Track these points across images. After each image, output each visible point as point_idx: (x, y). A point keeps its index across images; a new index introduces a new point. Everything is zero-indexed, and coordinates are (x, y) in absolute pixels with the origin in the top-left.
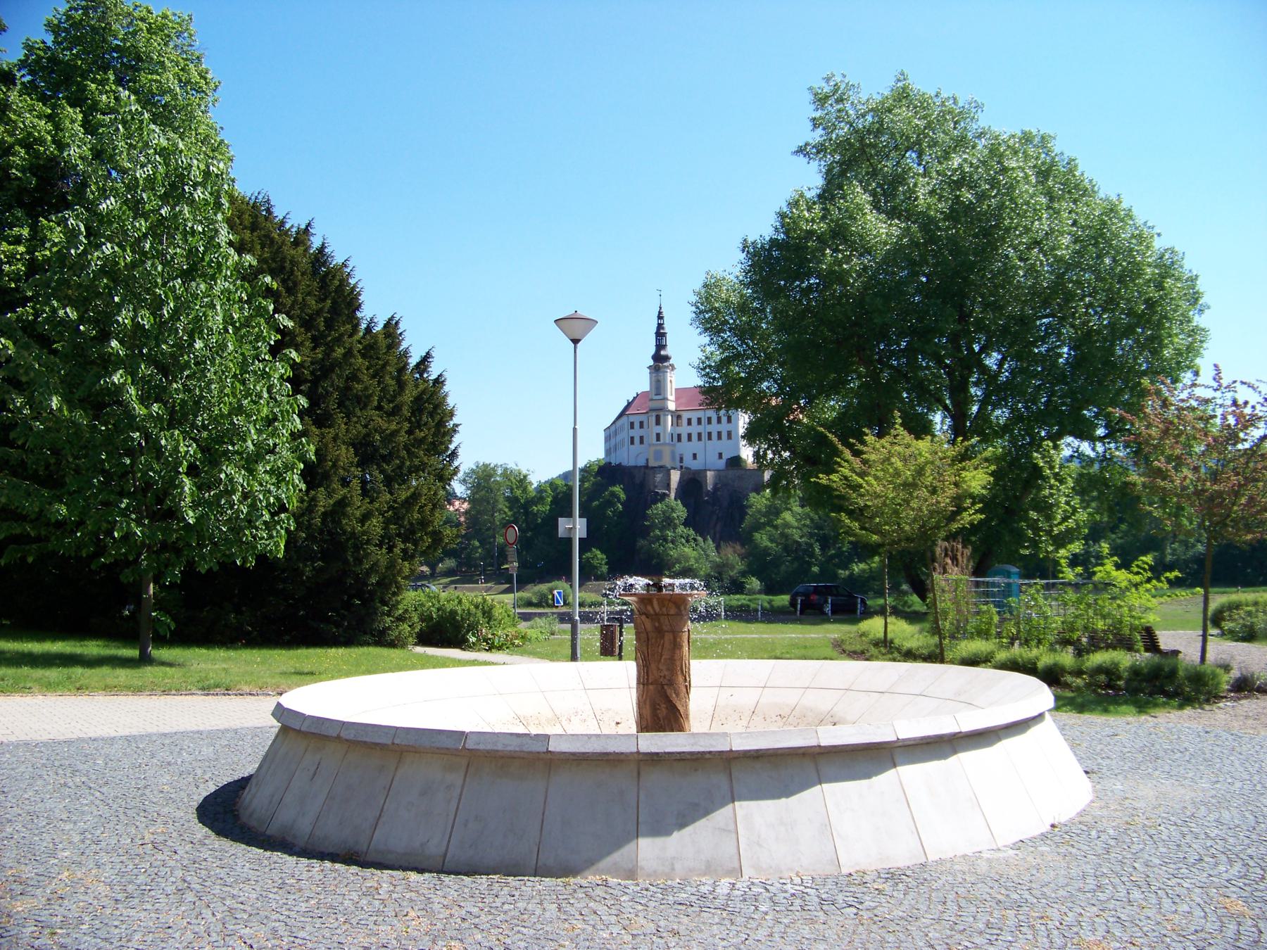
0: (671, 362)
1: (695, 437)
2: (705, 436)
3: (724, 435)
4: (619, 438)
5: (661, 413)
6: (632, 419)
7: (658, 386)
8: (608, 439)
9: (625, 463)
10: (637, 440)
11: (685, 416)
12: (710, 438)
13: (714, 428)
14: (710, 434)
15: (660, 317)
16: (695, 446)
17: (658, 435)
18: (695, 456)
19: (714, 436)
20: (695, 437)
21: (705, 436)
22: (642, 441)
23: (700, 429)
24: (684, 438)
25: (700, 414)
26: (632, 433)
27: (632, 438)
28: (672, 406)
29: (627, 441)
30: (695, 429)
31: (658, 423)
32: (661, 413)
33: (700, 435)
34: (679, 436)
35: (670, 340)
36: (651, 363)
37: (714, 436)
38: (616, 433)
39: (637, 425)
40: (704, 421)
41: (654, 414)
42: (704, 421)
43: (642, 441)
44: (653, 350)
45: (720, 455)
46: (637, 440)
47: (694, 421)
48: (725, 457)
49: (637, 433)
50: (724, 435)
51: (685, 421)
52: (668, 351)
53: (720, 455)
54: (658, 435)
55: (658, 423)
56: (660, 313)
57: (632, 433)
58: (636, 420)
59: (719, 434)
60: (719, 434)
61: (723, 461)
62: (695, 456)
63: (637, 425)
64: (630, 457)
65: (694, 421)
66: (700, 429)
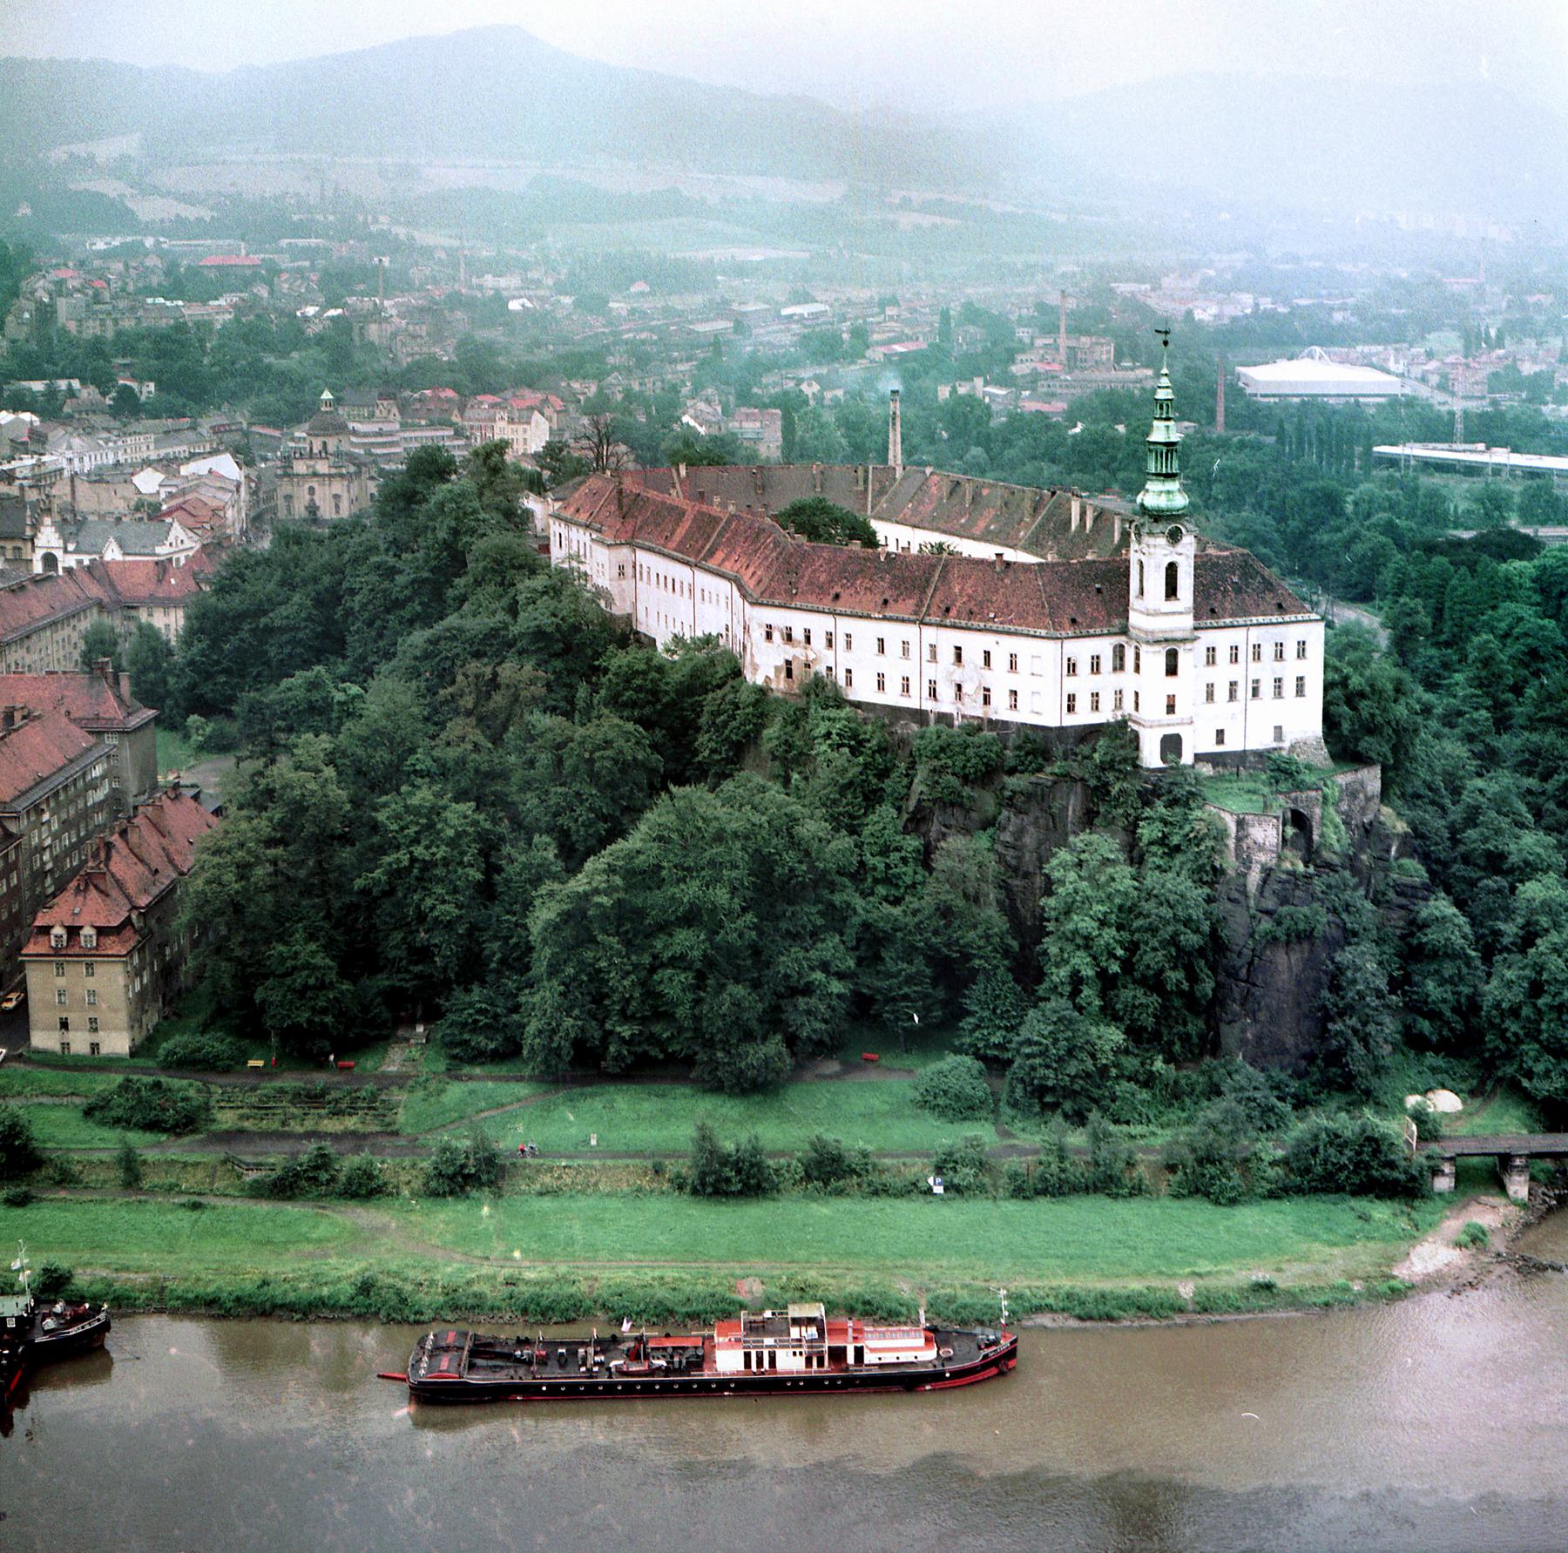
1: (1222, 692)
3: (1289, 687)
13: (1265, 671)
19: (1267, 688)
20: (1222, 692)
23: (1236, 672)
26: (1071, 684)
27: (1071, 698)
31: (1172, 670)
37: (1267, 688)
39: (1084, 667)
47: (1223, 655)
50: (1289, 687)
55: (1172, 670)
63: (1084, 667)
66: (1236, 672)
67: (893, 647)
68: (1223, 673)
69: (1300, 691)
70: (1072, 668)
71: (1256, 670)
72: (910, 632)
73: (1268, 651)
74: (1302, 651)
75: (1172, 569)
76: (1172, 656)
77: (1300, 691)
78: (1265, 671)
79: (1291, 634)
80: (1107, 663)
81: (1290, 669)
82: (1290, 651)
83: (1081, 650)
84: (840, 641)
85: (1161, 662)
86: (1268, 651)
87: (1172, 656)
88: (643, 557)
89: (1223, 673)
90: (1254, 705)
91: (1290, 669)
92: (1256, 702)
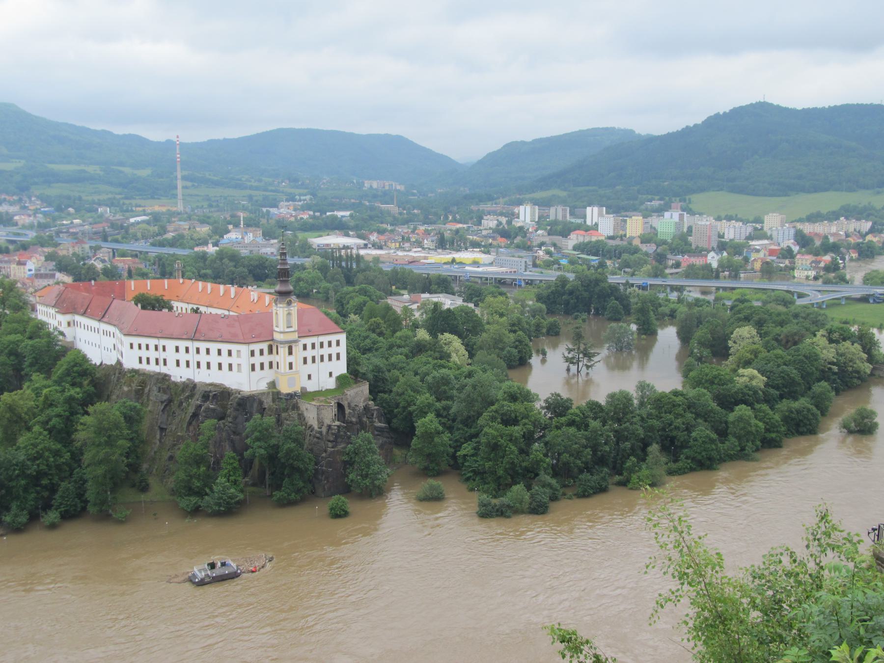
1: (309, 360)
2: (318, 359)
3: (334, 357)
5: (293, 345)
10: (258, 367)
13: (326, 351)
14: (322, 357)
16: (310, 368)
17: (291, 365)
18: (309, 377)
19: (326, 358)
20: (309, 360)
21: (318, 359)
26: (253, 360)
29: (246, 368)
31: (290, 353)
37: (326, 358)
39: (257, 353)
40: (317, 346)
42: (317, 346)
45: (331, 374)
46: (258, 367)
47: (309, 347)
48: (335, 375)
50: (334, 357)
53: (331, 374)
54: (291, 365)
55: (290, 353)
57: (253, 360)
59: (330, 356)
60: (330, 356)
61: (333, 379)
62: (309, 377)
63: (257, 353)
65: (309, 347)
67: (182, 350)
68: (309, 353)
69: (338, 358)
70: (252, 353)
72: (188, 343)
73: (326, 344)
75: (289, 314)
76: (290, 348)
77: (338, 358)
78: (326, 351)
79: (333, 338)
80: (266, 351)
81: (334, 350)
82: (334, 344)
83: (257, 347)
84: (160, 348)
86: (326, 344)
87: (290, 348)
88: (78, 318)
89: (309, 353)
91: (334, 350)
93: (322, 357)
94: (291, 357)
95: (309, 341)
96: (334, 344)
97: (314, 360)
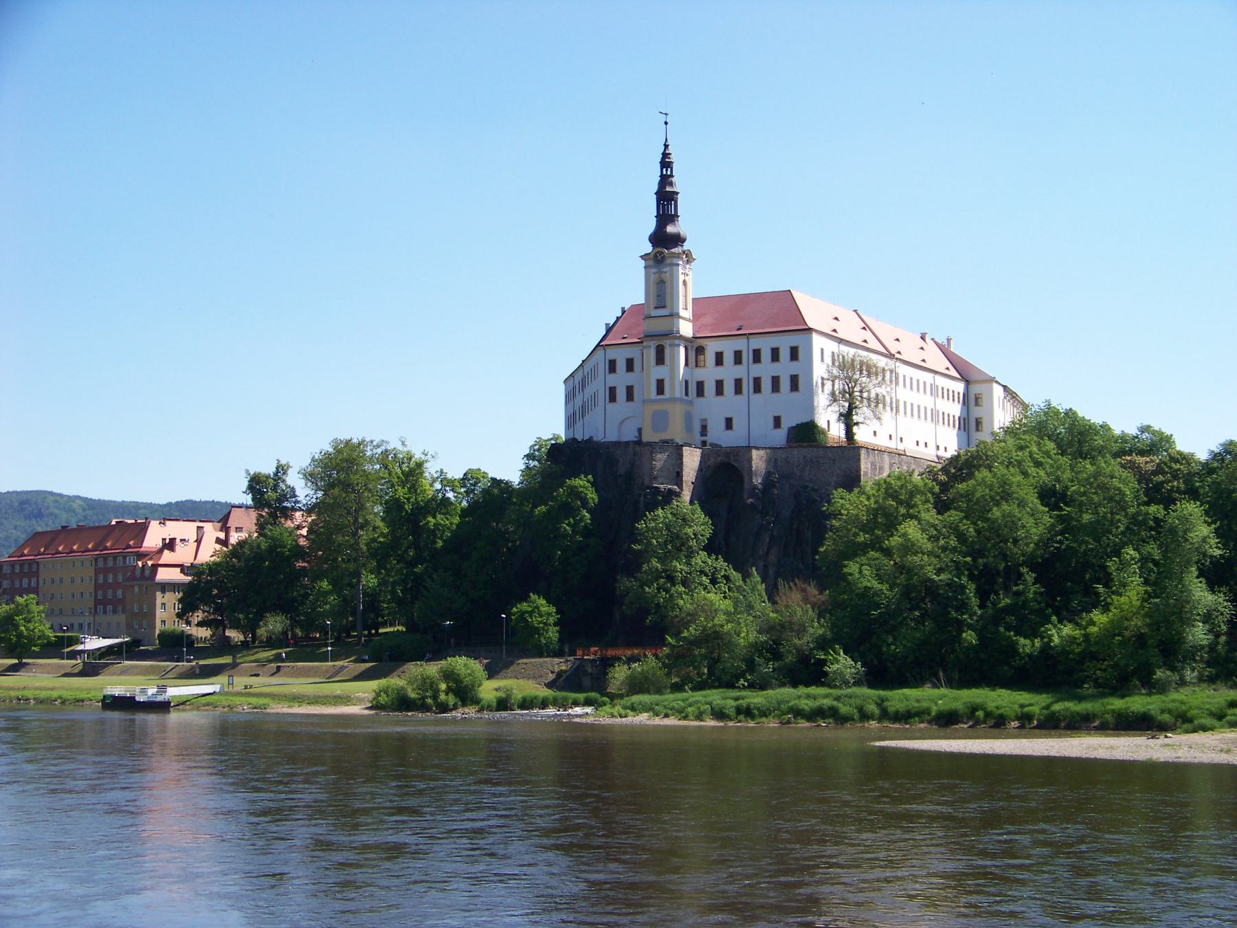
0: (686, 246)
1: (729, 387)
2: (747, 386)
3: (785, 384)
4: (589, 390)
5: (666, 343)
6: (612, 354)
7: (661, 291)
8: (570, 396)
9: (599, 437)
10: (621, 394)
11: (712, 348)
12: (757, 388)
13: (766, 370)
15: (666, 163)
16: (730, 404)
18: (729, 423)
19: (766, 385)
20: (729, 387)
21: (747, 386)
22: (630, 396)
23: (740, 371)
24: (710, 388)
25: (740, 344)
26: (612, 380)
28: (686, 329)
29: (603, 395)
30: (729, 372)
31: (660, 360)
32: (666, 343)
33: (738, 383)
34: (700, 387)
35: (684, 206)
36: (649, 248)
37: (766, 385)
38: (583, 384)
39: (621, 366)
40: (747, 357)
41: (653, 344)
42: (747, 357)
43: (630, 396)
44: (651, 225)
45: (777, 422)
46: (621, 394)
47: (728, 358)
48: (787, 423)
49: (621, 379)
50: (785, 384)
51: (710, 357)
52: (681, 227)
53: (777, 422)
55: (660, 360)
56: (665, 155)
57: (612, 380)
58: (620, 356)
59: (776, 381)
60: (776, 381)
62: (729, 423)
63: (621, 366)
64: (611, 424)
65: (728, 358)
66: (740, 371)
71: (756, 370)
73: (766, 355)
74: (794, 354)
78: (766, 370)
81: (785, 368)
82: (785, 354)
85: (653, 353)
86: (766, 355)
90: (755, 398)
91: (785, 368)
92: (757, 396)
93: (757, 384)
94: (660, 368)
95: (728, 348)
96: (785, 354)
97: (738, 388)
